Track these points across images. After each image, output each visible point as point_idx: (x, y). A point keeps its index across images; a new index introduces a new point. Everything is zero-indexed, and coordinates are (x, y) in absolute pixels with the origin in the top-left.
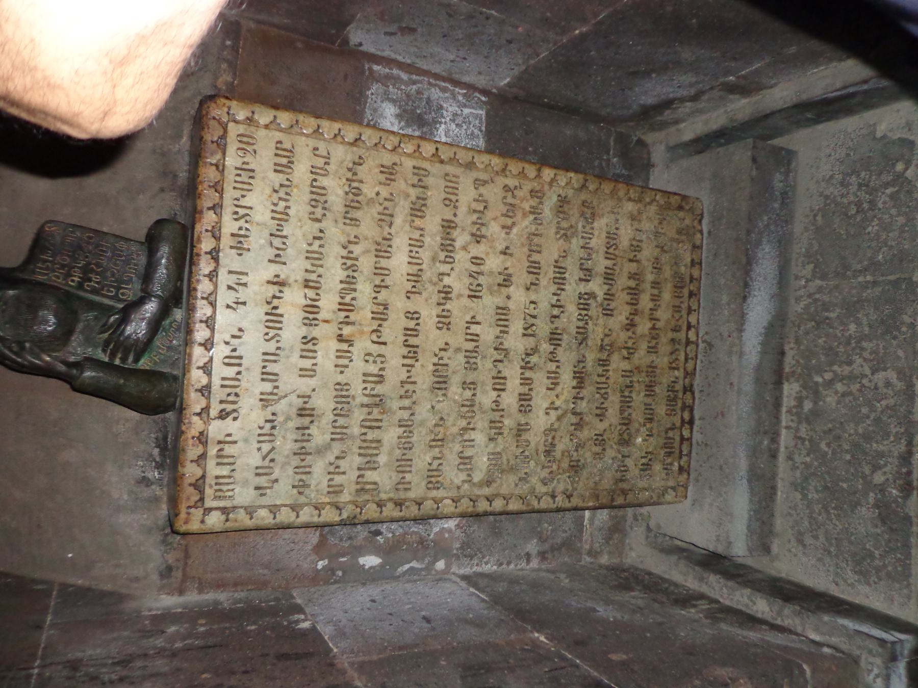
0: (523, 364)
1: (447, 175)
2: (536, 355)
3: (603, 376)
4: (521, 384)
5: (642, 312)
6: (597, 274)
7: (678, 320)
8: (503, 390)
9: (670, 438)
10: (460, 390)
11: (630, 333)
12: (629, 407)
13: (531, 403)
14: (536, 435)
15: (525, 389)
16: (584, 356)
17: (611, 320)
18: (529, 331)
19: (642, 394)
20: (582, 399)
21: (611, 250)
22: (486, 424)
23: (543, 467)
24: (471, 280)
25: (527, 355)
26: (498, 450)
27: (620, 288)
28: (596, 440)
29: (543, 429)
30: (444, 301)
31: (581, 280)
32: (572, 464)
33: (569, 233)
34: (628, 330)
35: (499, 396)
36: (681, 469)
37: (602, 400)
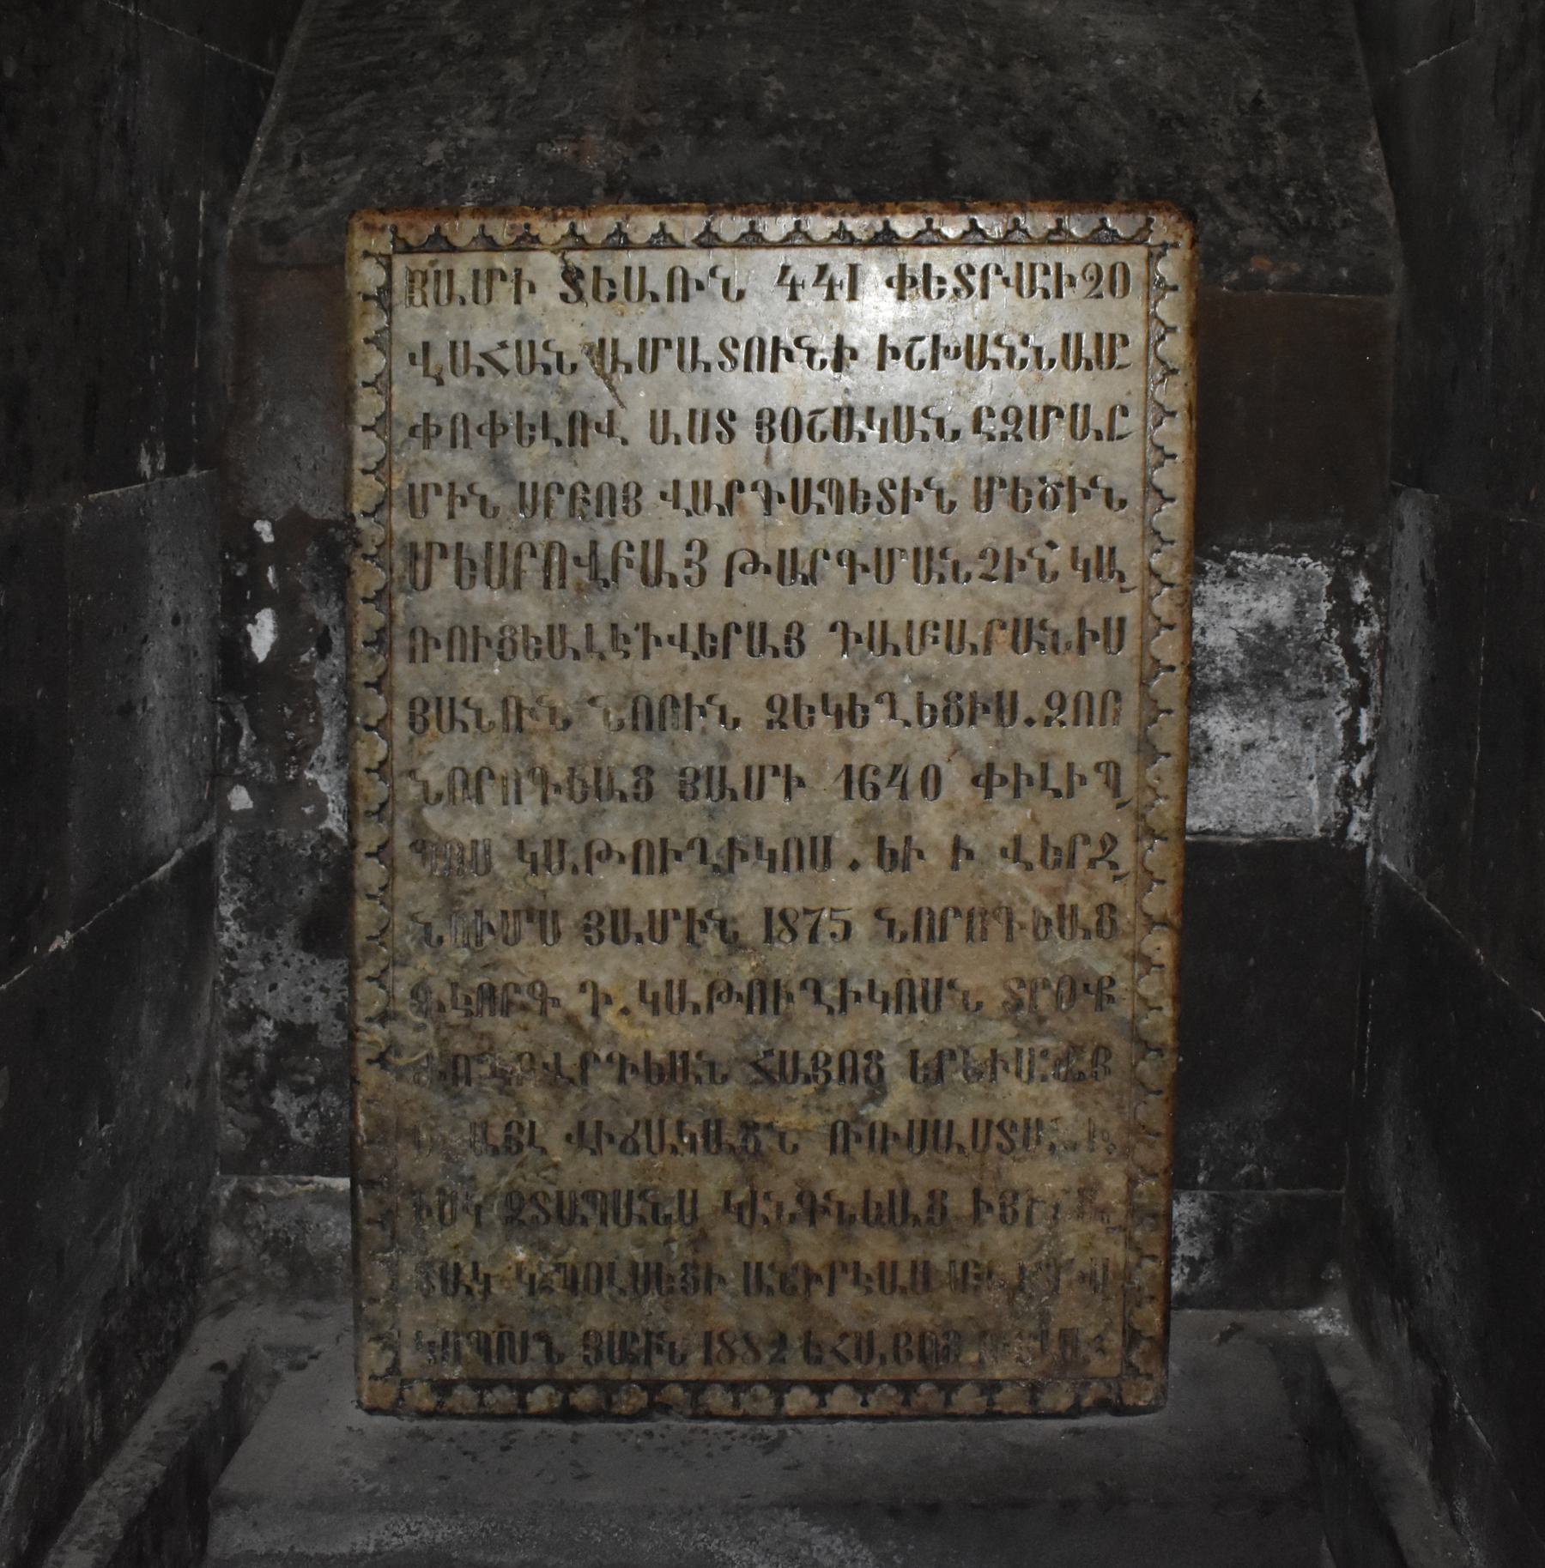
0: (700, 914)
1: (1118, 697)
2: (722, 947)
3: (680, 1135)
4: (652, 913)
5: (848, 1239)
6: (932, 1097)
7: (835, 1352)
8: (636, 870)
9: (525, 1348)
10: (633, 761)
11: (791, 1206)
12: (604, 1221)
13: (607, 943)
14: (532, 959)
15: (639, 925)
16: (725, 1078)
17: (822, 1149)
18: (778, 925)
19: (637, 1254)
20: (621, 1079)
21: (996, 1136)
22: (556, 831)
23: (454, 985)
24: (886, 771)
25: (722, 925)
26: (497, 865)
27: (904, 1168)
28: (521, 1128)
29: (544, 978)
30: (832, 709)
31: (914, 1054)
32: (462, 1062)
33: (1023, 1014)
34: (799, 1199)
35: (622, 858)
36: (443, 1388)
37: (619, 1139)
